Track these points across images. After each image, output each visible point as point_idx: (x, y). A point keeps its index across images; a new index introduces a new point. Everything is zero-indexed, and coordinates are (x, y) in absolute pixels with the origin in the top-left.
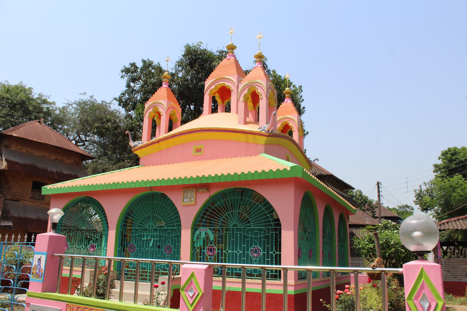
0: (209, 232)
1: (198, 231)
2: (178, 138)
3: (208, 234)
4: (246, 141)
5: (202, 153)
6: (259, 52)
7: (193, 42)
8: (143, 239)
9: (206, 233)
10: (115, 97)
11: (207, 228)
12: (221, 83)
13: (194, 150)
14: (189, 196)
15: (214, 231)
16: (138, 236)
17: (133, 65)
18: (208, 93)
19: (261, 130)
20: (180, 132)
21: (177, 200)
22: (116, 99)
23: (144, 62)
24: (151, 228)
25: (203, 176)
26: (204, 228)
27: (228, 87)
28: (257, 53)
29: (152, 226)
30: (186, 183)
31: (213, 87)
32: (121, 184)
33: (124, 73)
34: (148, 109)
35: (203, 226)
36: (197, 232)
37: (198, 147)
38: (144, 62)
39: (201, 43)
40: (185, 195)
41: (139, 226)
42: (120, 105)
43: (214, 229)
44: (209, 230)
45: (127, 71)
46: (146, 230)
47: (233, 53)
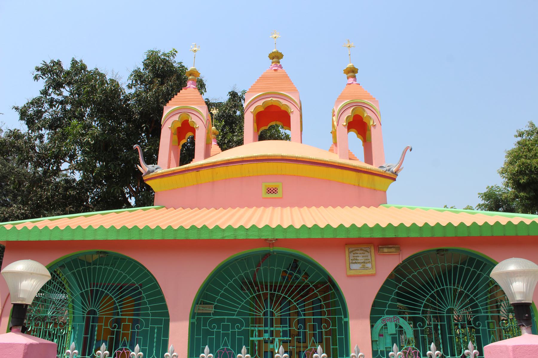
0: (403, 323)
1: (379, 321)
2: (238, 167)
3: (401, 327)
4: (357, 184)
5: (279, 194)
6: (351, 64)
7: (163, 48)
8: (251, 339)
9: (396, 325)
10: (16, 106)
11: (398, 316)
12: (274, 99)
13: (264, 190)
14: (361, 259)
15: (414, 321)
16: (240, 334)
17: (59, 63)
18: (252, 109)
19: (385, 169)
20: (243, 158)
21: (335, 267)
22: (17, 109)
23: (74, 63)
24: (269, 317)
25: (402, 225)
26: (392, 316)
27: (283, 108)
28: (350, 65)
29: (272, 314)
30: (354, 235)
31: (260, 103)
32: (212, 231)
33: (39, 73)
34: (172, 114)
35: (388, 313)
36: (379, 324)
37: (272, 185)
38: (74, 63)
39: (176, 51)
40: (352, 258)
41: (239, 314)
42: (21, 119)
43: (410, 319)
44: (401, 320)
45: (44, 70)
46: (257, 321)
47: (279, 63)
